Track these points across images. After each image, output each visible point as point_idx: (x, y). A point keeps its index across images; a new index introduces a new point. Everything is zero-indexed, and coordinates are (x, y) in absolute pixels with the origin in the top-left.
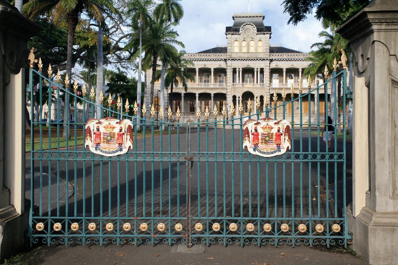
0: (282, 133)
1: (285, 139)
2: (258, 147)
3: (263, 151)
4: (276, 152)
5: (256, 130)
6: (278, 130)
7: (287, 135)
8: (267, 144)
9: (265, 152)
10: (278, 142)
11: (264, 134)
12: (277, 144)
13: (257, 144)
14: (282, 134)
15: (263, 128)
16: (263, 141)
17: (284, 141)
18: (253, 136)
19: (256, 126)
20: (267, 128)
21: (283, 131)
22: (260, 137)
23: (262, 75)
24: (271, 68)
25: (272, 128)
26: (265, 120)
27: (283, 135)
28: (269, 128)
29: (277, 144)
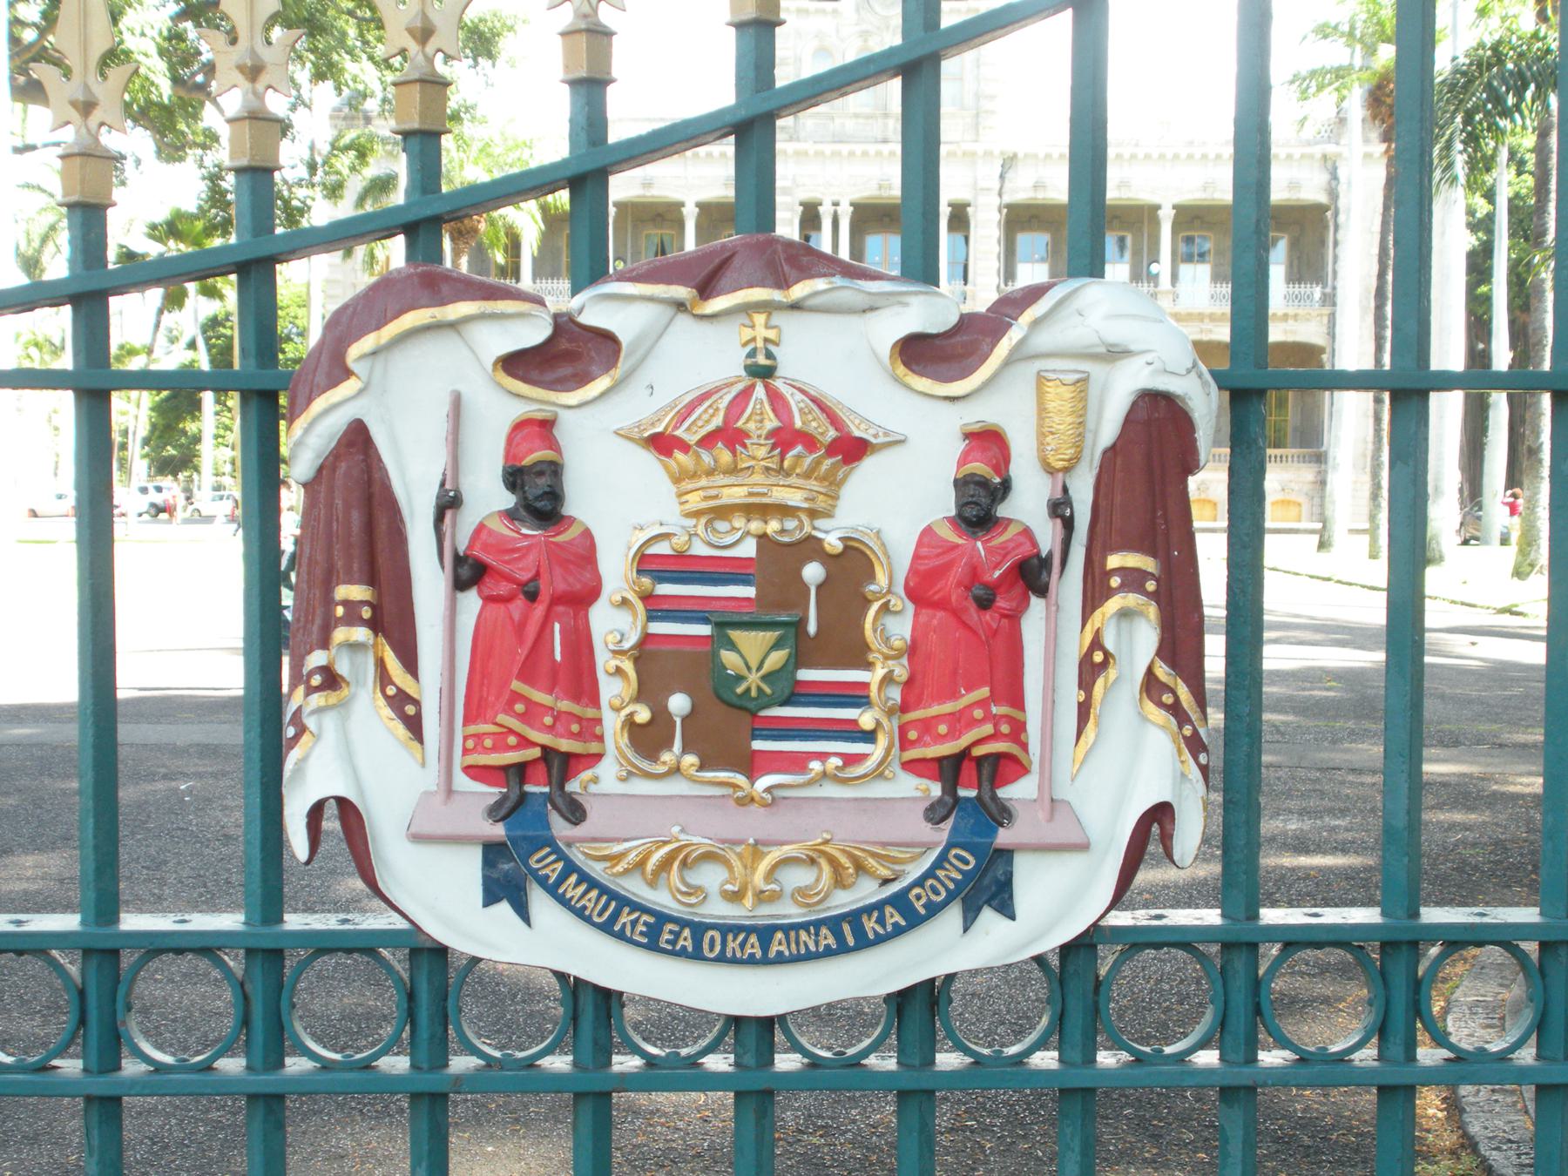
0: (1047, 536)
1: (1091, 669)
2: (575, 812)
3: (661, 899)
4: (914, 921)
5: (538, 490)
6: (962, 484)
7: (1134, 580)
8: (752, 765)
9: (718, 910)
10: (960, 721)
11: (682, 567)
12: (950, 770)
13: (562, 765)
14: (1032, 575)
15: (662, 444)
16: (679, 703)
17: (1084, 711)
18: (471, 602)
19: (531, 400)
20: (760, 450)
21: (1060, 509)
22: (613, 625)
23: (959, 237)
24: (1007, 199)
25: (852, 450)
26: (706, 289)
27: (1070, 585)
28: (785, 438)
29: (950, 770)
